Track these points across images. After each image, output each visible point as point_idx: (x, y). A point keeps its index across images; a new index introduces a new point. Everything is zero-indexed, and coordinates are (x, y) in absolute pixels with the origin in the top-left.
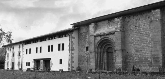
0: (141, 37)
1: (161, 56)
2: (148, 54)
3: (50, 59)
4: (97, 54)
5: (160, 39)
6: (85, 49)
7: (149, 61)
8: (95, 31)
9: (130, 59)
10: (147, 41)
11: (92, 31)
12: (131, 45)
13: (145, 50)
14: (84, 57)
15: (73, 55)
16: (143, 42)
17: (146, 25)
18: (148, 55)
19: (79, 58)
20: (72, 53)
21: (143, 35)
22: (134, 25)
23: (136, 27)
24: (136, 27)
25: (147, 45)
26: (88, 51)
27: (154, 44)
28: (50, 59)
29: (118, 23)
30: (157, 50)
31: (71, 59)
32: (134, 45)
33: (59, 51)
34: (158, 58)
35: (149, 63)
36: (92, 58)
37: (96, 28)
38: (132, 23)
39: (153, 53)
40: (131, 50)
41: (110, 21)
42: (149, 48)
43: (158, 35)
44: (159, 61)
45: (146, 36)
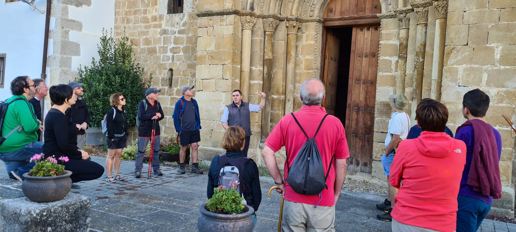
4: (247, 33)
14: (152, 51)
15: (73, 36)
20: (70, 17)
26: (176, 17)
31: (59, 56)
36: (214, 57)
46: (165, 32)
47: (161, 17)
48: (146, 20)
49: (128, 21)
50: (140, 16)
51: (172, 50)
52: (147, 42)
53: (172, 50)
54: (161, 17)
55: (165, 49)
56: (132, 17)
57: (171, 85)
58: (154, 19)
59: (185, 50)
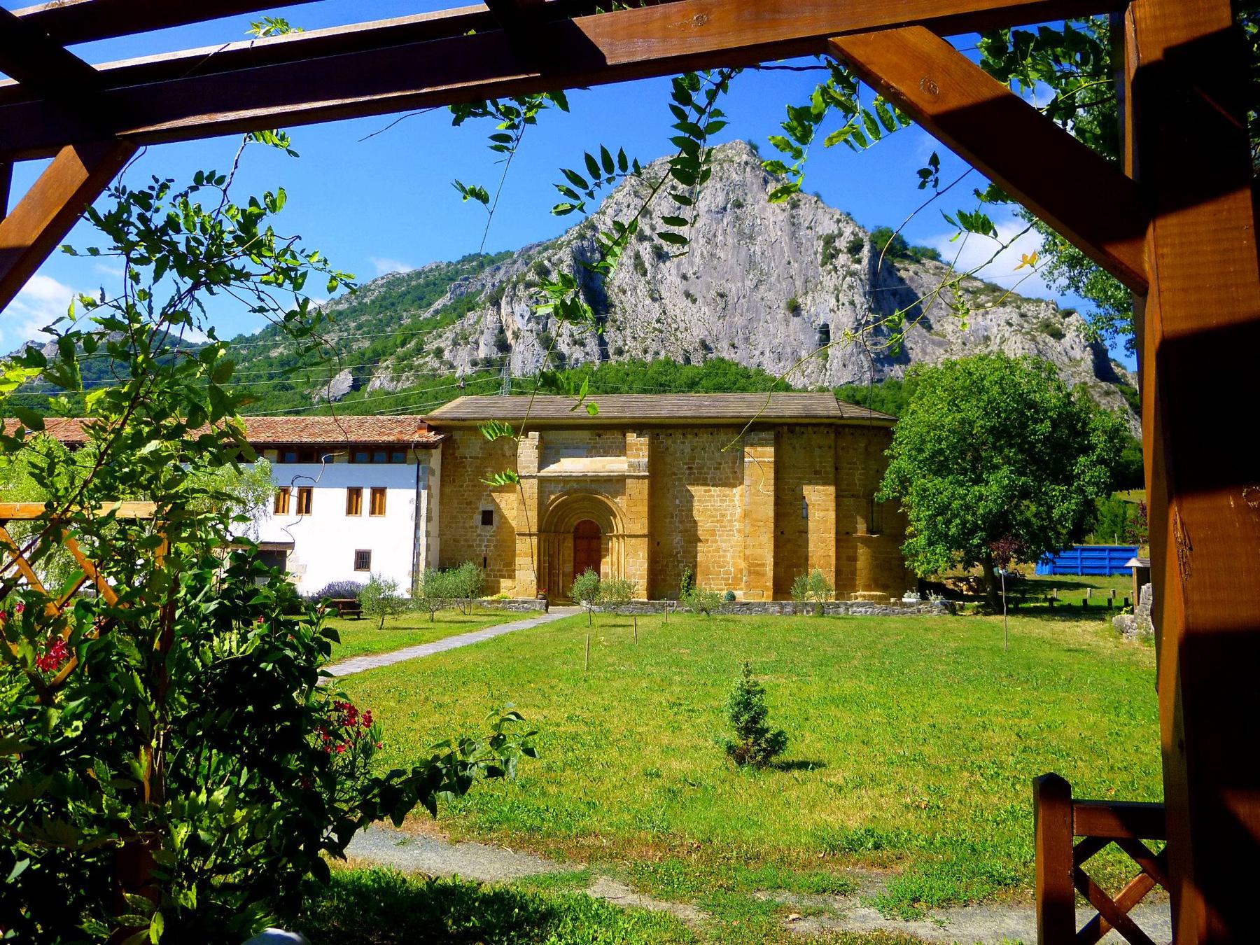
0: (707, 501)
1: (769, 560)
2: (725, 551)
3: (291, 545)
5: (771, 514)
6: (478, 518)
7: (727, 573)
8: (542, 464)
9: (667, 566)
10: (724, 515)
11: (532, 462)
12: (670, 523)
13: (716, 541)
16: (711, 516)
17: (724, 469)
18: (724, 556)
19: (441, 550)
21: (713, 496)
22: (686, 464)
23: (690, 468)
24: (690, 468)
25: (724, 527)
26: (488, 527)
27: (753, 526)
28: (291, 545)
29: (641, 450)
30: (760, 544)
32: (681, 522)
33: (352, 518)
34: (763, 565)
35: (727, 579)
36: (526, 555)
37: (547, 455)
38: (678, 454)
39: (748, 552)
40: (671, 535)
41: (600, 436)
42: (730, 535)
43: (766, 503)
44: (764, 575)
45: (722, 501)
46: (480, 535)
47: (477, 527)
48: (464, 528)
49: (451, 527)
50: (461, 525)
51: (486, 546)
52: (466, 541)
53: (486, 546)
54: (477, 527)
55: (480, 546)
56: (454, 525)
57: (485, 567)
58: (472, 527)
59: (494, 546)
